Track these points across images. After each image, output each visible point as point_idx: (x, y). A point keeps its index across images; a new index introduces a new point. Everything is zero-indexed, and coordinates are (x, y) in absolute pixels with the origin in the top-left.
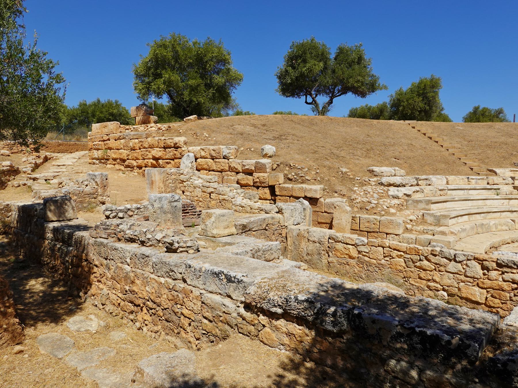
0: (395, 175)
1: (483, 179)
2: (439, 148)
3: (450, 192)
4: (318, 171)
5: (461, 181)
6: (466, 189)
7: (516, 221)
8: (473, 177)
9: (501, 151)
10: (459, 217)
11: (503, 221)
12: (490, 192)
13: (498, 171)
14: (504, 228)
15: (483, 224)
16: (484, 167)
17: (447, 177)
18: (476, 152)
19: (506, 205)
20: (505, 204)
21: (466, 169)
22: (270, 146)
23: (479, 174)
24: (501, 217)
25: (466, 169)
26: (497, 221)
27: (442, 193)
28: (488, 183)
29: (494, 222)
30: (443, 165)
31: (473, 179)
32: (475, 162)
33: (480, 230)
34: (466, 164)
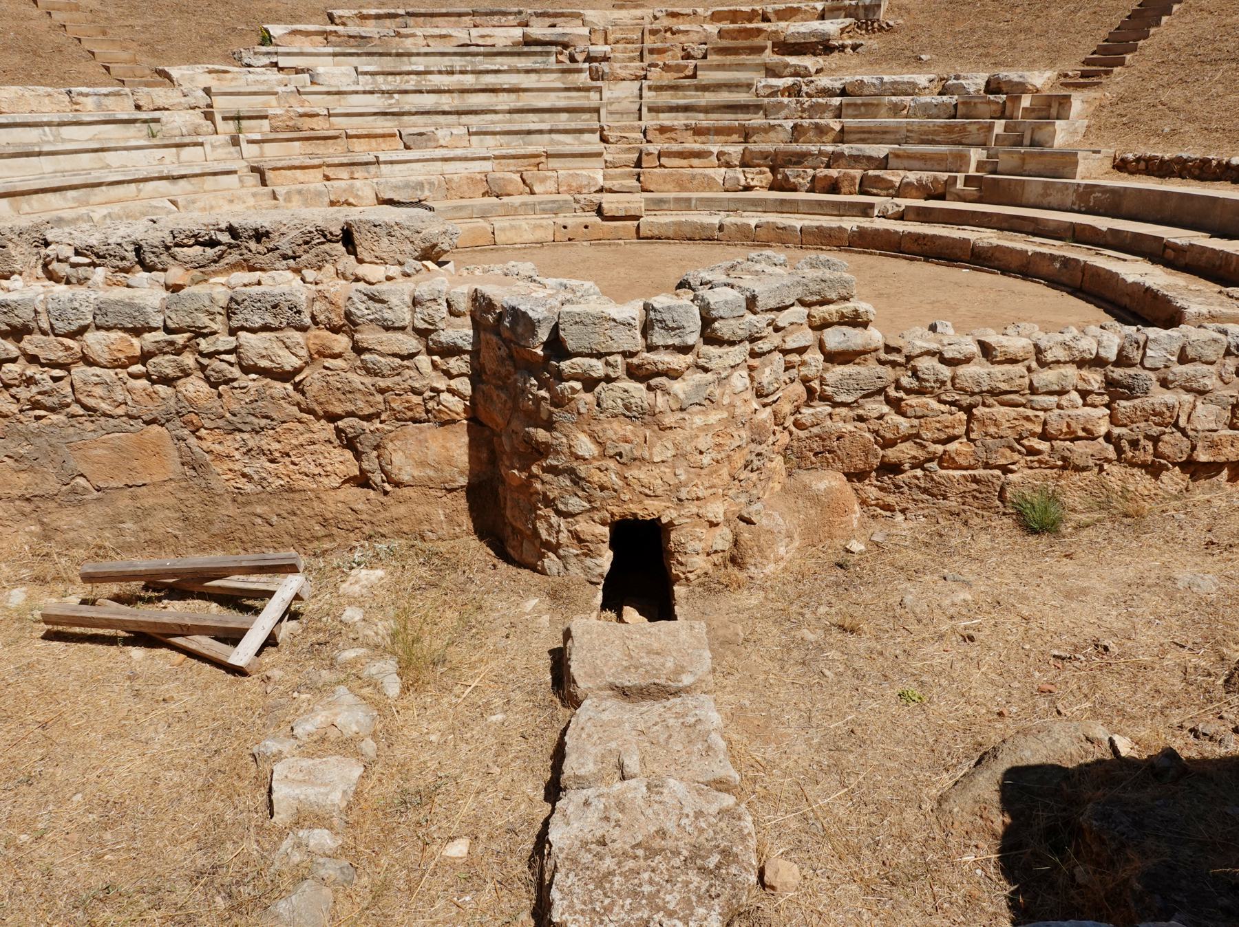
2: (23, 7)
5: (47, 100)
6: (49, 124)
7: (180, 204)
8: (84, 90)
9: (210, 21)
11: (135, 206)
12: (132, 130)
13: (175, 72)
16: (147, 62)
18: (139, 22)
19: (170, 161)
20: (167, 161)
21: (94, 68)
23: (123, 81)
24: (142, 195)
25: (94, 68)
26: (116, 208)
28: (138, 107)
29: (104, 211)
30: (17, 59)
31: (87, 95)
32: (126, 49)
34: (93, 54)
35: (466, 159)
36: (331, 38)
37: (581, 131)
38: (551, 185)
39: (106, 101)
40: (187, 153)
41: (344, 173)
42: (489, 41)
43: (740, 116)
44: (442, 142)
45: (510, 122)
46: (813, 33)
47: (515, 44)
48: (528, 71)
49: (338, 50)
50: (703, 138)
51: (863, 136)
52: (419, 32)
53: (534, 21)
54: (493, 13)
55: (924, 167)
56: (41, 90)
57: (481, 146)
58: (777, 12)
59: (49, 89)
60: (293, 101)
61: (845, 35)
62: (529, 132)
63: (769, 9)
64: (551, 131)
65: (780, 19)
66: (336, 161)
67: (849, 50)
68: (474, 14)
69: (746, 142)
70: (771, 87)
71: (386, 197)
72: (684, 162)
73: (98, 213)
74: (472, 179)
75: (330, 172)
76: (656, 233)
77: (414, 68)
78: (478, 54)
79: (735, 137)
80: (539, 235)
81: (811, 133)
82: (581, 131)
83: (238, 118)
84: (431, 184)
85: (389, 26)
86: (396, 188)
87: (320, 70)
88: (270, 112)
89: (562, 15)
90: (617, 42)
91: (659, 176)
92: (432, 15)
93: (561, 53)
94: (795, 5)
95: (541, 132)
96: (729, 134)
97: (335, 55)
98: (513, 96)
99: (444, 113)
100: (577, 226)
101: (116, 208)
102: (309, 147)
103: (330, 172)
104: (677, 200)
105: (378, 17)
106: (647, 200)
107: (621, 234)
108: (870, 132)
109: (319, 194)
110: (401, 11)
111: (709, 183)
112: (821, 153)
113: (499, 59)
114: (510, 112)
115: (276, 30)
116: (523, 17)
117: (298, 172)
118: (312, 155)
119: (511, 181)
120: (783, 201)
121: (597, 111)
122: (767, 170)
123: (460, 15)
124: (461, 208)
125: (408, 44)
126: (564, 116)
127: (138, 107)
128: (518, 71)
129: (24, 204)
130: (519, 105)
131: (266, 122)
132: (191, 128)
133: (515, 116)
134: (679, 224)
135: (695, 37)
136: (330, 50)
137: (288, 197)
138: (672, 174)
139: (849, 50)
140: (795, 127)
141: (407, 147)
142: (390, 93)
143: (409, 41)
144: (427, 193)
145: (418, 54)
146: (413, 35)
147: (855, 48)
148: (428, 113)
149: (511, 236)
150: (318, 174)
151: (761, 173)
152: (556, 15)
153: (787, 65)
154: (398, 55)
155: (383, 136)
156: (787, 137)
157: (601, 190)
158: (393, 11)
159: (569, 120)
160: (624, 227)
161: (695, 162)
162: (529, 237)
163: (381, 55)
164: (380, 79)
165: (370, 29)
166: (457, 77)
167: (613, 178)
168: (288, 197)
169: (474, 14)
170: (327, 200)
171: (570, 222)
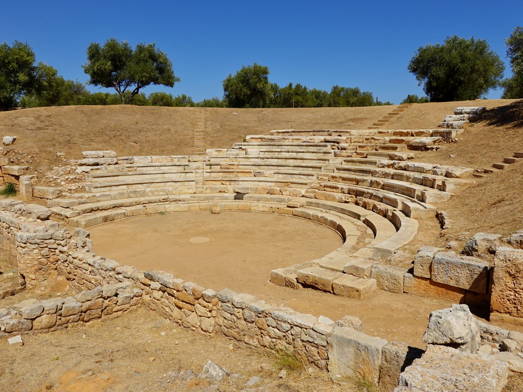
0: (103, 157)
1: (184, 158)
3: (138, 168)
4: (35, 155)
6: (157, 166)
8: (174, 157)
10: (113, 187)
14: (161, 193)
15: (136, 191)
17: (153, 157)
22: (7, 137)
26: (154, 189)
27: (130, 169)
33: (131, 195)
35: (266, 182)
36: (263, 140)
37: (309, 175)
38: (288, 193)
39: (181, 159)
40: (188, 175)
41: (228, 183)
42: (313, 141)
43: (365, 174)
44: (266, 175)
45: (294, 170)
46: (421, 143)
47: (321, 142)
48: (313, 152)
49: (259, 143)
50: (345, 182)
51: (389, 188)
52: (290, 138)
53: (333, 134)
54: (319, 131)
55: (390, 204)
56: (164, 157)
57: (276, 178)
58: (416, 133)
59: (166, 157)
60: (234, 160)
61: (436, 144)
62: (293, 174)
63: (413, 132)
64: (299, 174)
65: (417, 136)
66: (225, 179)
67: (434, 150)
68: (314, 131)
69: (357, 185)
70: (382, 164)
71: (237, 191)
72: (331, 190)
73: (148, 190)
74: (263, 188)
75: (223, 182)
76: (297, 214)
77: (277, 150)
78: (303, 146)
79: (354, 182)
80: (264, 209)
81: (375, 185)
82: (309, 175)
83: (211, 165)
84: (251, 188)
85: (281, 136)
86: (240, 189)
87: (249, 150)
88: (221, 163)
89: (342, 132)
90: (355, 142)
91: (320, 194)
92: (300, 132)
93: (334, 145)
94: (422, 130)
95: (296, 174)
96: (353, 181)
97: (259, 145)
98: (302, 161)
99: (273, 166)
100: (275, 208)
101: (154, 189)
102: (225, 174)
103: (223, 182)
104: (316, 203)
105: (283, 132)
106: (307, 202)
107: (288, 213)
108: (390, 187)
109: (216, 189)
110: (290, 130)
111: (334, 199)
112: (368, 193)
113: (310, 147)
114: (294, 166)
115: (248, 137)
116: (329, 133)
117: (214, 182)
118: (226, 177)
119: (276, 190)
120: (342, 209)
121: (320, 168)
122: (354, 196)
123: (309, 132)
124: (252, 197)
125: (287, 143)
126: (311, 169)
127: (189, 161)
128: (310, 152)
129: (131, 187)
130: (297, 164)
131: (219, 166)
132: (197, 167)
133: (295, 168)
134: (302, 212)
135: (381, 142)
136: (257, 144)
137: (206, 189)
138: (323, 194)
139: (434, 150)
140: (371, 181)
141: (255, 176)
142: (263, 158)
143: (287, 140)
144: (249, 191)
145: (284, 145)
146: (288, 139)
147: (437, 149)
148: (268, 165)
149: (255, 208)
150: (220, 183)
151: (352, 197)
152: (340, 132)
153: (396, 156)
154: (278, 145)
155: (248, 172)
156: (369, 185)
157: (303, 196)
158: (287, 130)
159: (312, 171)
160: (290, 210)
161: (334, 190)
162: (261, 209)
163: (273, 145)
164: (267, 153)
165: (275, 137)
166: (290, 153)
167: (309, 192)
168: (206, 189)
169: (314, 131)
170: (218, 190)
171: (273, 206)
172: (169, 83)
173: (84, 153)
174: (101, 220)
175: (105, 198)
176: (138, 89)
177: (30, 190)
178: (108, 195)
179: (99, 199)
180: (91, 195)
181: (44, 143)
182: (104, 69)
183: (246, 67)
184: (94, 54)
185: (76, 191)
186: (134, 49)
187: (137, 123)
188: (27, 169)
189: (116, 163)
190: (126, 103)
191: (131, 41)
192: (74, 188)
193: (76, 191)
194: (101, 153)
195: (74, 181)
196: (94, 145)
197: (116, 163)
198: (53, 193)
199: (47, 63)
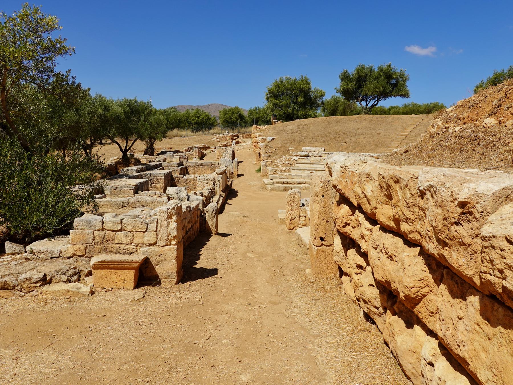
172: (405, 95)
173: (303, 148)
174: (283, 189)
175: (298, 177)
176: (378, 101)
177: (265, 169)
178: (300, 175)
179: (293, 177)
180: (288, 174)
181: (286, 142)
182: (348, 89)
183: (499, 71)
184: (345, 77)
185: (285, 171)
186: (376, 70)
187: (358, 129)
188: (269, 156)
189: (321, 156)
190: (365, 114)
191: (374, 62)
192: (284, 169)
193: (285, 171)
194: (313, 149)
195: (287, 165)
196: (316, 143)
197: (321, 156)
198: (271, 171)
199: (319, 88)
